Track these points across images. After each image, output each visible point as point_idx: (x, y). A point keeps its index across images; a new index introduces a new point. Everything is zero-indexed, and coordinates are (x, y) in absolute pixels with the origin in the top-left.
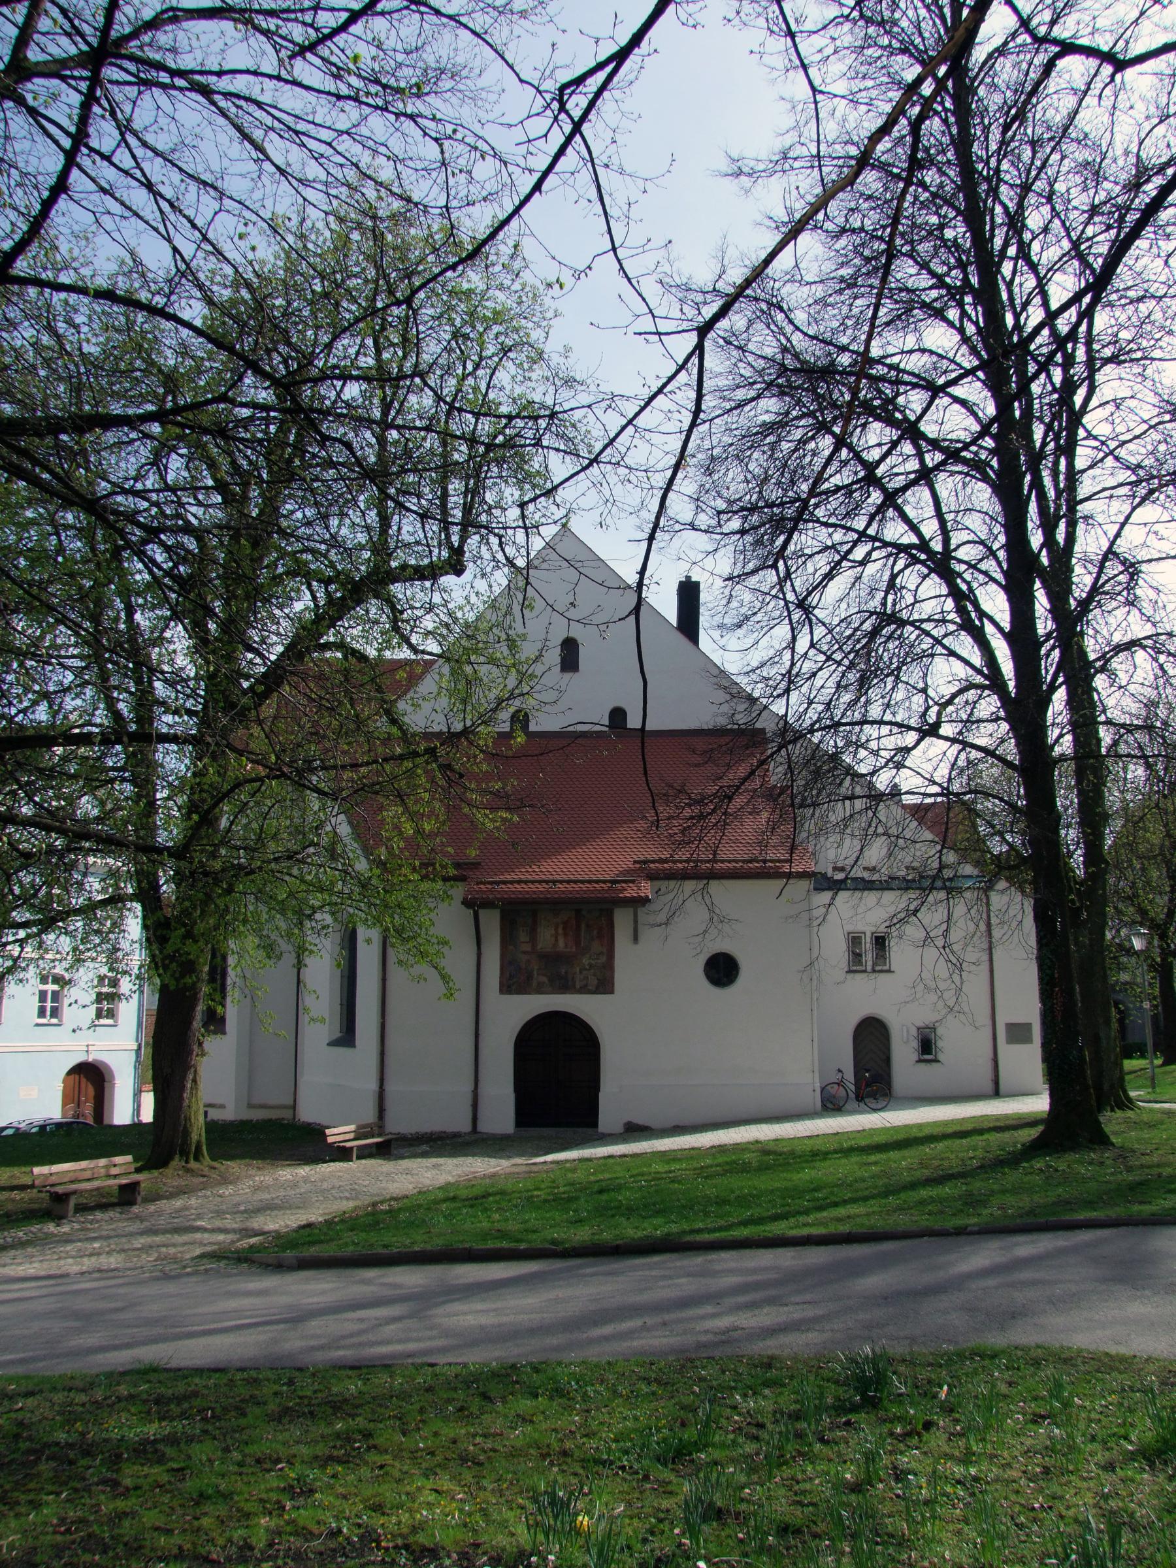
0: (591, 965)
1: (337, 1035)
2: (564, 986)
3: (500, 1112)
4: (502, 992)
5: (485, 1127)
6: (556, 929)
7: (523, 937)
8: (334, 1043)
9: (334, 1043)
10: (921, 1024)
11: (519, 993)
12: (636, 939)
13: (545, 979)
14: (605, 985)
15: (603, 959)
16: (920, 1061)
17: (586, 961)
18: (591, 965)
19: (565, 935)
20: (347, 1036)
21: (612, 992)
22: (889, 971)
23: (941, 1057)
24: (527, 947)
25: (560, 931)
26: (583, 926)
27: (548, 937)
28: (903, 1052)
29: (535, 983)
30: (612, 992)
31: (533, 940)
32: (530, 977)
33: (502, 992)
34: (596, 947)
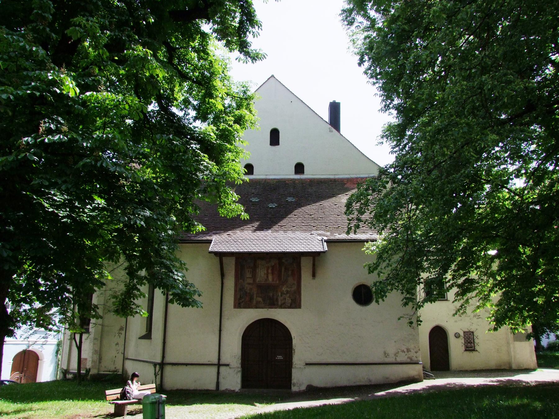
0: (287, 292)
1: (144, 333)
2: (273, 304)
3: (233, 380)
4: (235, 307)
5: (222, 388)
6: (267, 271)
7: (248, 275)
8: (142, 338)
9: (142, 338)
10: (466, 330)
11: (245, 307)
12: (314, 275)
13: (260, 299)
14: (296, 304)
15: (294, 288)
16: (466, 350)
17: (284, 289)
18: (287, 292)
19: (273, 273)
20: (148, 336)
21: (299, 306)
22: (447, 300)
23: (477, 348)
24: (251, 281)
25: (270, 271)
26: (283, 270)
27: (263, 274)
28: (456, 347)
29: (254, 302)
30: (299, 306)
31: (254, 276)
32: (251, 299)
33: (235, 307)
34: (290, 280)
